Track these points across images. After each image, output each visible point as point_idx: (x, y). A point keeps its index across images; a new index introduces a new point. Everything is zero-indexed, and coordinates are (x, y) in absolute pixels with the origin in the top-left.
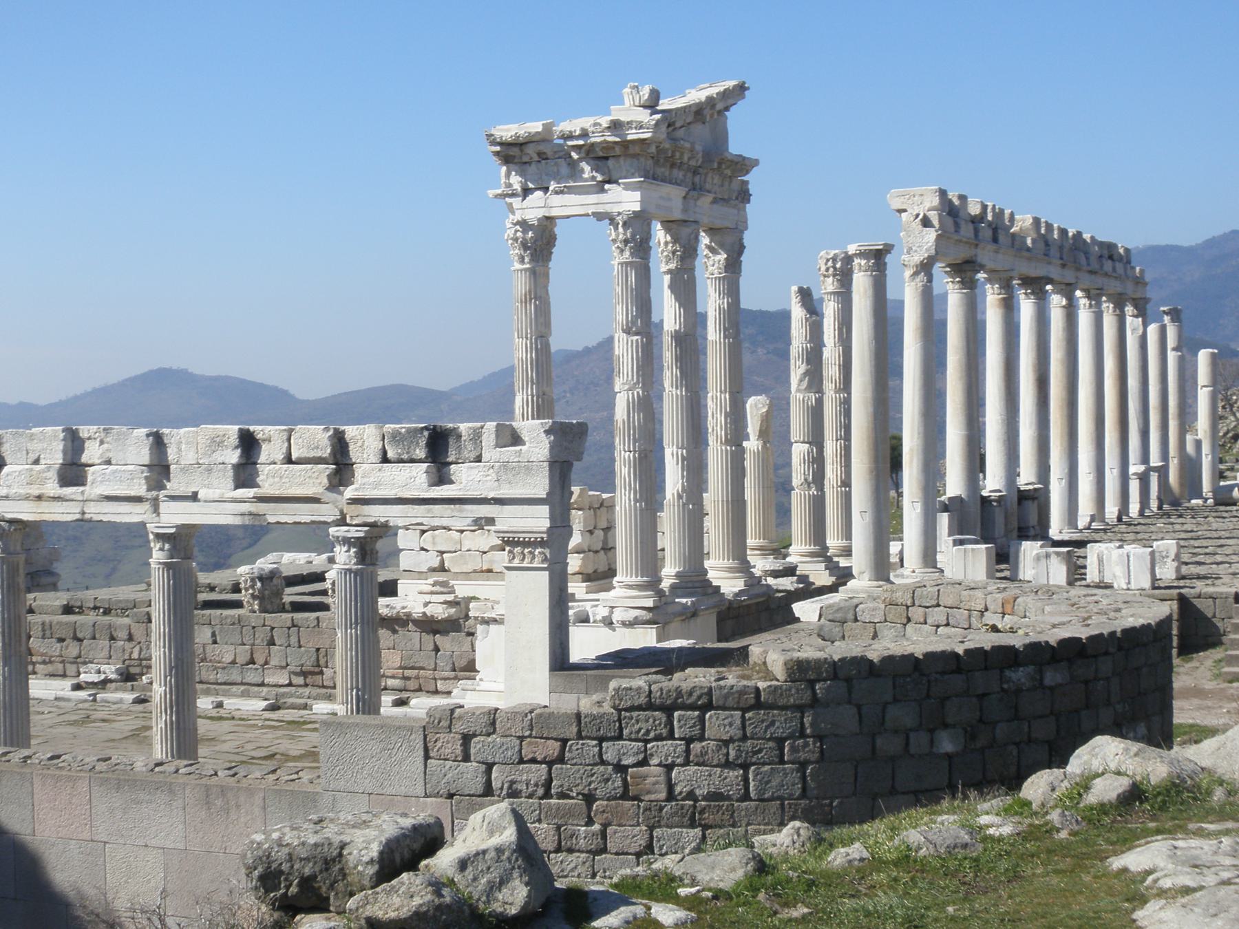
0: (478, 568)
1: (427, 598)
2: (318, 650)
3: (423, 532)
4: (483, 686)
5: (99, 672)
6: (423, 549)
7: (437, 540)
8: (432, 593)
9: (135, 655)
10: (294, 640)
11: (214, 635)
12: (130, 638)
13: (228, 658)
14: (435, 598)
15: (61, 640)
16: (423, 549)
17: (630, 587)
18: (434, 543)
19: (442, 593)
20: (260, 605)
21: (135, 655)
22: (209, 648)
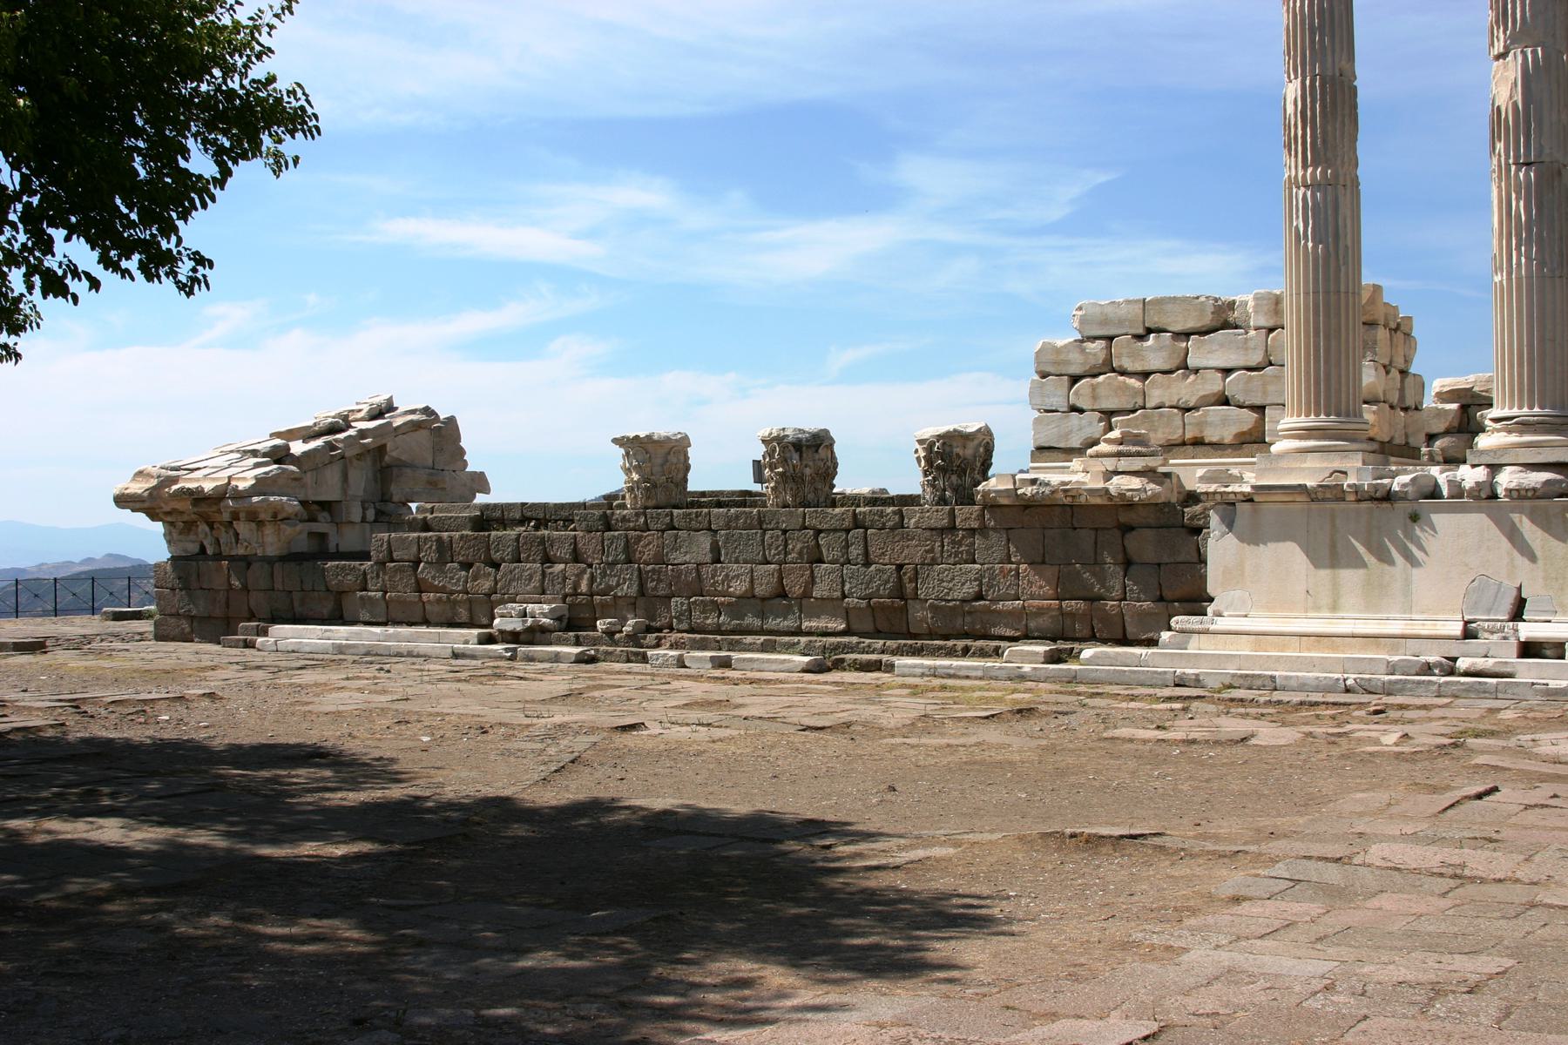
0: (1176, 436)
1: (1110, 464)
2: (900, 567)
3: (1075, 379)
4: (1222, 624)
5: (524, 614)
6: (1074, 409)
7: (1102, 391)
8: (1119, 455)
9: (584, 587)
10: (855, 552)
11: (716, 550)
12: (576, 557)
13: (739, 587)
14: (1124, 464)
15: (467, 566)
16: (1074, 409)
17: (1525, 426)
18: (1095, 398)
19: (1139, 454)
20: (794, 496)
21: (584, 587)
22: (706, 571)
